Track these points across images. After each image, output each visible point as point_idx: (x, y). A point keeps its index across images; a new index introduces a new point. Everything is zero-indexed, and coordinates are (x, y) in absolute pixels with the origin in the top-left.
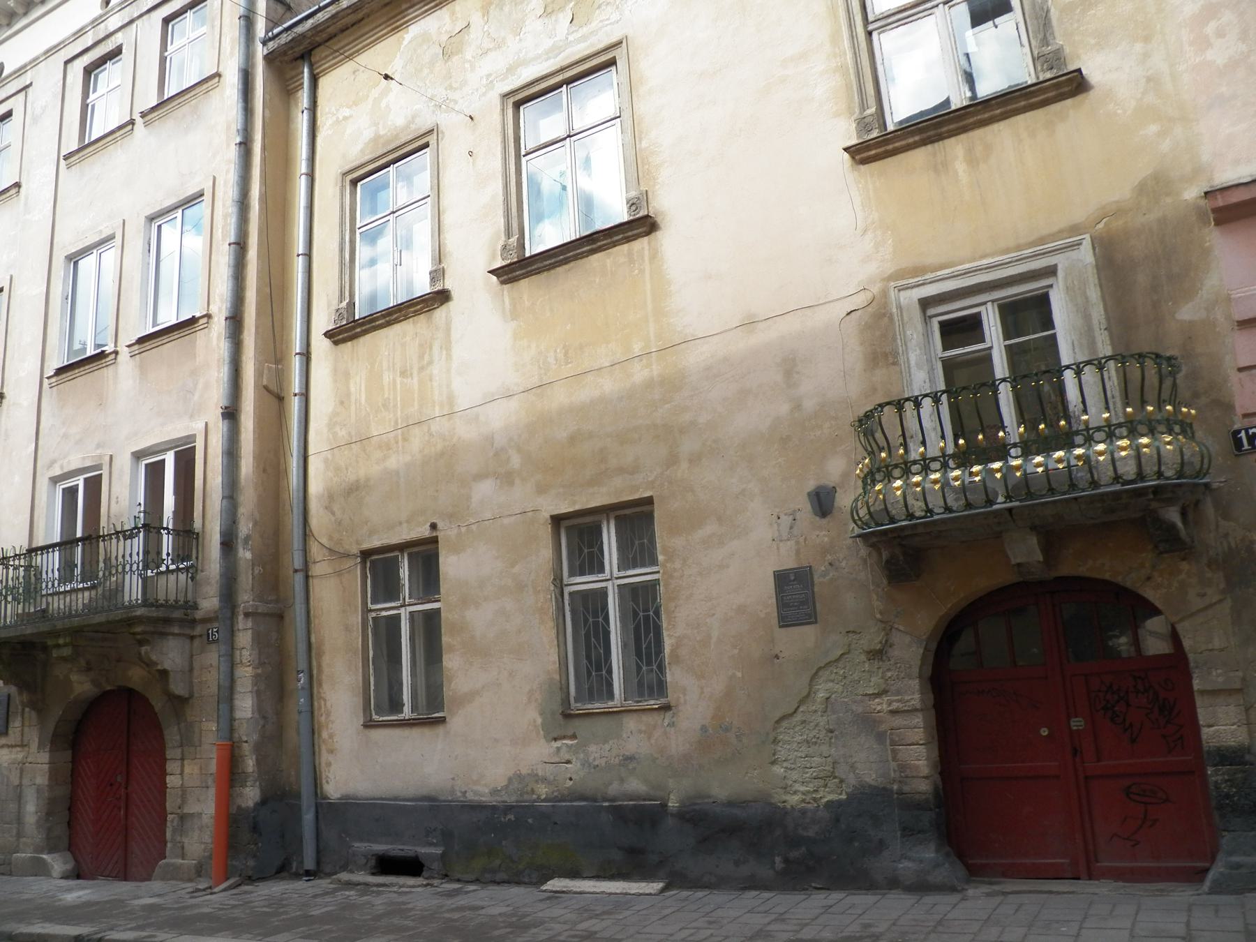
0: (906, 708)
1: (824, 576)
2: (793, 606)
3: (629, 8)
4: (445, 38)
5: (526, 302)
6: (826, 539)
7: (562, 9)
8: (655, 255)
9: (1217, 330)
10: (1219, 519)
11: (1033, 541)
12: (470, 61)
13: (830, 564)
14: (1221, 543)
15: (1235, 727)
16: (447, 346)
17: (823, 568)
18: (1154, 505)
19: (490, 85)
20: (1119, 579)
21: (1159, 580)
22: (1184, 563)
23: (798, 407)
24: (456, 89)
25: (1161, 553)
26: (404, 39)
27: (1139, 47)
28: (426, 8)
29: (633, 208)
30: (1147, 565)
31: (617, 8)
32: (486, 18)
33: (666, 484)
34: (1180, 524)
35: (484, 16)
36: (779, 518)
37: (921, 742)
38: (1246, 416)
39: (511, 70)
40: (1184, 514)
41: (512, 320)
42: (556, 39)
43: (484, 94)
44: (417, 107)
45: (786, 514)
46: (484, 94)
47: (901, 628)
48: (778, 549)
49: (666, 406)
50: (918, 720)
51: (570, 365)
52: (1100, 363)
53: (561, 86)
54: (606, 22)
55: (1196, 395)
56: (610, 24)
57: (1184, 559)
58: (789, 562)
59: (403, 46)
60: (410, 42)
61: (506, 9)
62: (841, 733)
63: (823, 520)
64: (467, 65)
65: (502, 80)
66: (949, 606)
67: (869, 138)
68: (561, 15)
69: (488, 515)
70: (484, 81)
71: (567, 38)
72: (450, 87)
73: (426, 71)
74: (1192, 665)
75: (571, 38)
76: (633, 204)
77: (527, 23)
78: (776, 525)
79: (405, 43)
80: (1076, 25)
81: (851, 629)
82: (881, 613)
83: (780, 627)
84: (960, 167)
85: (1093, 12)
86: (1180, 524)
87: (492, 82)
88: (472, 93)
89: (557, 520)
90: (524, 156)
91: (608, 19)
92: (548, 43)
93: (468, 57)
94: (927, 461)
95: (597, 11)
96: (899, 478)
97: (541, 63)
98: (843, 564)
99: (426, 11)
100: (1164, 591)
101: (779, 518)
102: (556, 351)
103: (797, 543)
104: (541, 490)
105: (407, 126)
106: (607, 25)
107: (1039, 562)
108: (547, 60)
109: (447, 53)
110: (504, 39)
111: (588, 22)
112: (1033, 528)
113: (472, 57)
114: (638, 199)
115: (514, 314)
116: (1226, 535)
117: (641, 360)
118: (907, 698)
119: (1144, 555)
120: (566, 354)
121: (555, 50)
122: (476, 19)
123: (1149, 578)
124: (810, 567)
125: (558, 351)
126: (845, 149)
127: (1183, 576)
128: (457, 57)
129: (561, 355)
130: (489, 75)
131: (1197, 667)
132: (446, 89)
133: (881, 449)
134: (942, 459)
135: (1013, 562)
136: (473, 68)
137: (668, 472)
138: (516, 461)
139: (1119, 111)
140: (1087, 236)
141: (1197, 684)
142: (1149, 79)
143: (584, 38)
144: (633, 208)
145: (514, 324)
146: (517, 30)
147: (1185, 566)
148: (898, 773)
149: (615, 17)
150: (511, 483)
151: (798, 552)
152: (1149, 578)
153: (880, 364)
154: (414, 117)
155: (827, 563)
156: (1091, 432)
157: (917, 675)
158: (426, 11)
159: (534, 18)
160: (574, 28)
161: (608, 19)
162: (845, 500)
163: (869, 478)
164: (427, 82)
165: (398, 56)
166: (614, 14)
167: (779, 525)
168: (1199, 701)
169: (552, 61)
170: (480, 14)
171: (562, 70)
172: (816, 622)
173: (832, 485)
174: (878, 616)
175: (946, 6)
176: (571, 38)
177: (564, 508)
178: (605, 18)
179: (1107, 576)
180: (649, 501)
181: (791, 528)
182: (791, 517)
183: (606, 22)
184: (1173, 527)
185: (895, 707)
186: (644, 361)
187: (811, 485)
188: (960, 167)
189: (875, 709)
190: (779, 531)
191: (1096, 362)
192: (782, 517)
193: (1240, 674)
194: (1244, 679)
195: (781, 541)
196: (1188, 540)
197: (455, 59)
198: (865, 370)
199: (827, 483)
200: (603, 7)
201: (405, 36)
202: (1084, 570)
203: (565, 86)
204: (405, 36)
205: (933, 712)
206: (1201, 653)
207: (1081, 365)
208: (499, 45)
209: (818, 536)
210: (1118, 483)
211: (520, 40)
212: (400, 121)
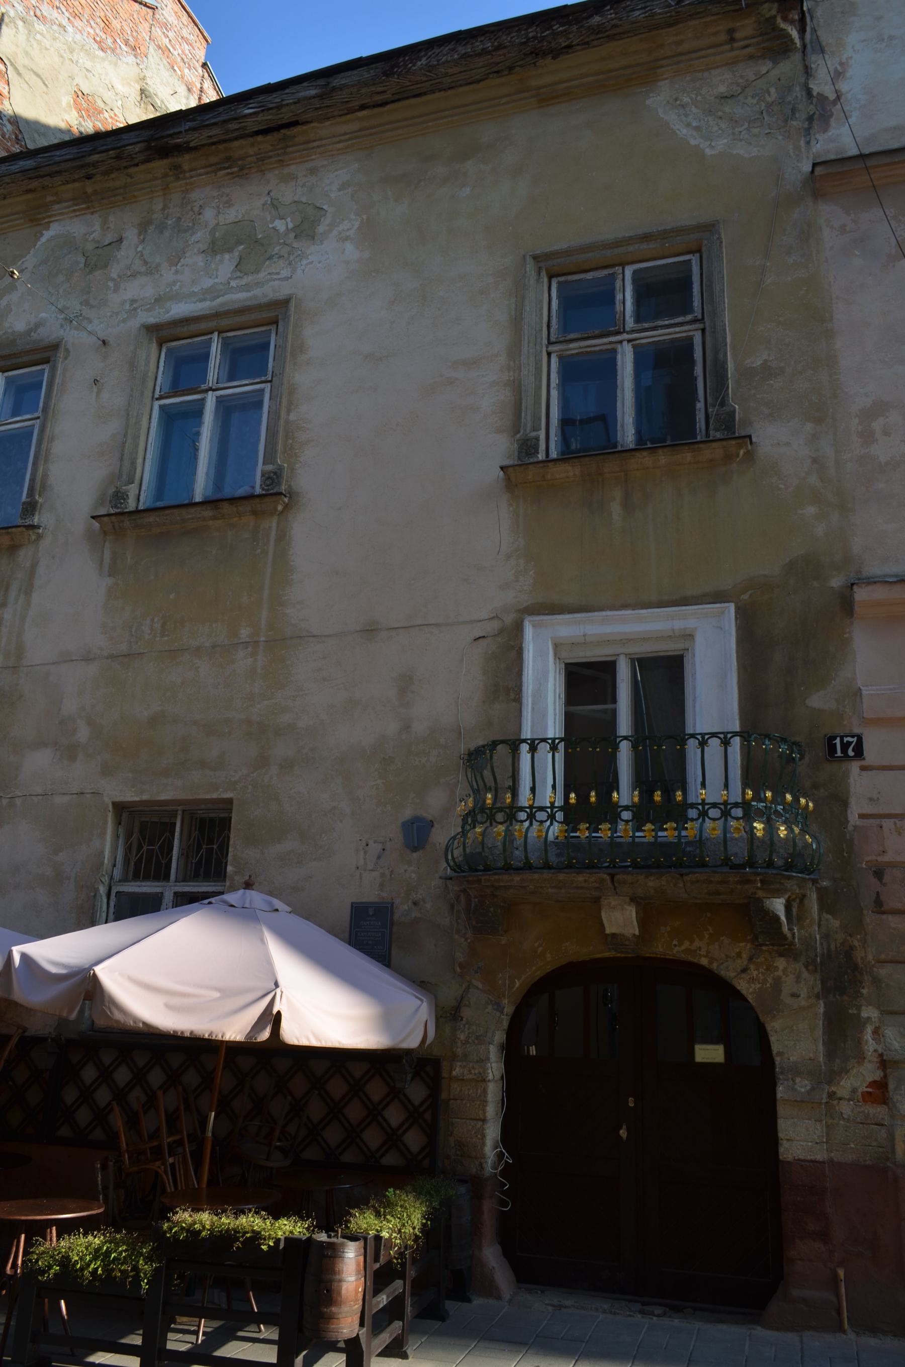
3: (303, 267)
4: (90, 247)
5: (129, 560)
6: (414, 875)
7: (230, 250)
8: (283, 537)
9: (845, 723)
11: (631, 912)
12: (113, 280)
13: (415, 904)
16: (28, 590)
17: (406, 907)
18: (760, 894)
19: (132, 313)
20: (714, 966)
21: (755, 973)
22: (782, 959)
23: (407, 728)
24: (92, 307)
26: (42, 235)
27: (809, 426)
28: (76, 208)
29: (268, 482)
30: (744, 956)
31: (290, 264)
32: (142, 237)
33: (250, 787)
34: (783, 918)
35: (140, 234)
36: (367, 845)
38: (862, 816)
39: (159, 300)
40: (788, 908)
41: (110, 576)
42: (216, 280)
43: (124, 321)
44: (44, 315)
45: (375, 842)
46: (124, 321)
47: (480, 986)
48: (361, 878)
49: (266, 702)
51: (166, 638)
52: (725, 737)
53: (212, 333)
54: (275, 277)
55: (816, 786)
56: (279, 279)
57: (781, 955)
58: (370, 893)
59: (39, 243)
60: (48, 240)
61: (167, 233)
63: (415, 855)
64: (111, 284)
65: (149, 310)
67: (529, 462)
68: (227, 256)
69: (39, 790)
70: (127, 306)
71: (229, 283)
72: (86, 303)
73: (61, 278)
75: (233, 284)
76: (269, 478)
77: (187, 255)
78: (362, 853)
79: (43, 240)
80: (753, 391)
84: (616, 509)
85: (772, 382)
86: (783, 918)
87: (135, 309)
88: (111, 316)
89: (120, 808)
90: (157, 399)
91: (278, 274)
92: (207, 283)
93: (114, 275)
94: (534, 810)
95: (267, 263)
96: (501, 823)
97: (195, 303)
98: (428, 906)
99: (75, 211)
100: (758, 986)
101: (367, 845)
102: (153, 620)
103: (383, 875)
104: (107, 771)
105: (28, 332)
106: (276, 279)
107: (634, 935)
108: (205, 300)
109: (91, 266)
110: (158, 266)
111: (257, 271)
112: (633, 900)
113: (119, 277)
114: (275, 473)
115: (113, 572)
117: (247, 648)
119: (741, 944)
120: (164, 625)
121: (211, 293)
122: (131, 235)
123: (745, 970)
124: (392, 904)
125: (156, 620)
126: (502, 468)
127: (780, 973)
128: (100, 272)
129: (158, 626)
130: (133, 301)
131: (782, 1073)
132: (81, 304)
133: (488, 789)
134: (549, 810)
135: (608, 931)
136: (116, 289)
137: (255, 774)
138: (83, 734)
139: (782, 486)
140: (732, 606)
142: (815, 460)
143: (246, 288)
144: (268, 482)
145: (110, 581)
146: (175, 260)
147: (781, 963)
149: (285, 273)
150: (73, 758)
151: (382, 885)
152: (745, 970)
153: (501, 698)
154: (37, 326)
155: (410, 903)
156: (707, 807)
158: (75, 211)
159: (195, 251)
160: (239, 274)
161: (278, 274)
162: (440, 837)
163: (470, 818)
164: (61, 291)
165: (32, 252)
166: (285, 270)
167: (365, 853)
168: (781, 1110)
169: (207, 304)
170: (136, 231)
171: (217, 315)
173: (430, 818)
175: (630, 344)
176: (233, 284)
177: (130, 796)
178: (274, 271)
179: (704, 962)
180: (230, 801)
181: (379, 857)
182: (380, 847)
183: (275, 277)
184: (777, 918)
186: (250, 649)
187: (408, 813)
188: (616, 509)
190: (365, 859)
191: (722, 736)
192: (371, 843)
195: (365, 870)
196: (789, 935)
197: (98, 273)
198: (484, 702)
199: (425, 815)
200: (275, 259)
201: (44, 232)
202: (679, 950)
203: (216, 334)
204: (44, 232)
207: (707, 737)
208: (152, 270)
209: (405, 871)
210: (727, 865)
211: (177, 272)
212: (20, 326)
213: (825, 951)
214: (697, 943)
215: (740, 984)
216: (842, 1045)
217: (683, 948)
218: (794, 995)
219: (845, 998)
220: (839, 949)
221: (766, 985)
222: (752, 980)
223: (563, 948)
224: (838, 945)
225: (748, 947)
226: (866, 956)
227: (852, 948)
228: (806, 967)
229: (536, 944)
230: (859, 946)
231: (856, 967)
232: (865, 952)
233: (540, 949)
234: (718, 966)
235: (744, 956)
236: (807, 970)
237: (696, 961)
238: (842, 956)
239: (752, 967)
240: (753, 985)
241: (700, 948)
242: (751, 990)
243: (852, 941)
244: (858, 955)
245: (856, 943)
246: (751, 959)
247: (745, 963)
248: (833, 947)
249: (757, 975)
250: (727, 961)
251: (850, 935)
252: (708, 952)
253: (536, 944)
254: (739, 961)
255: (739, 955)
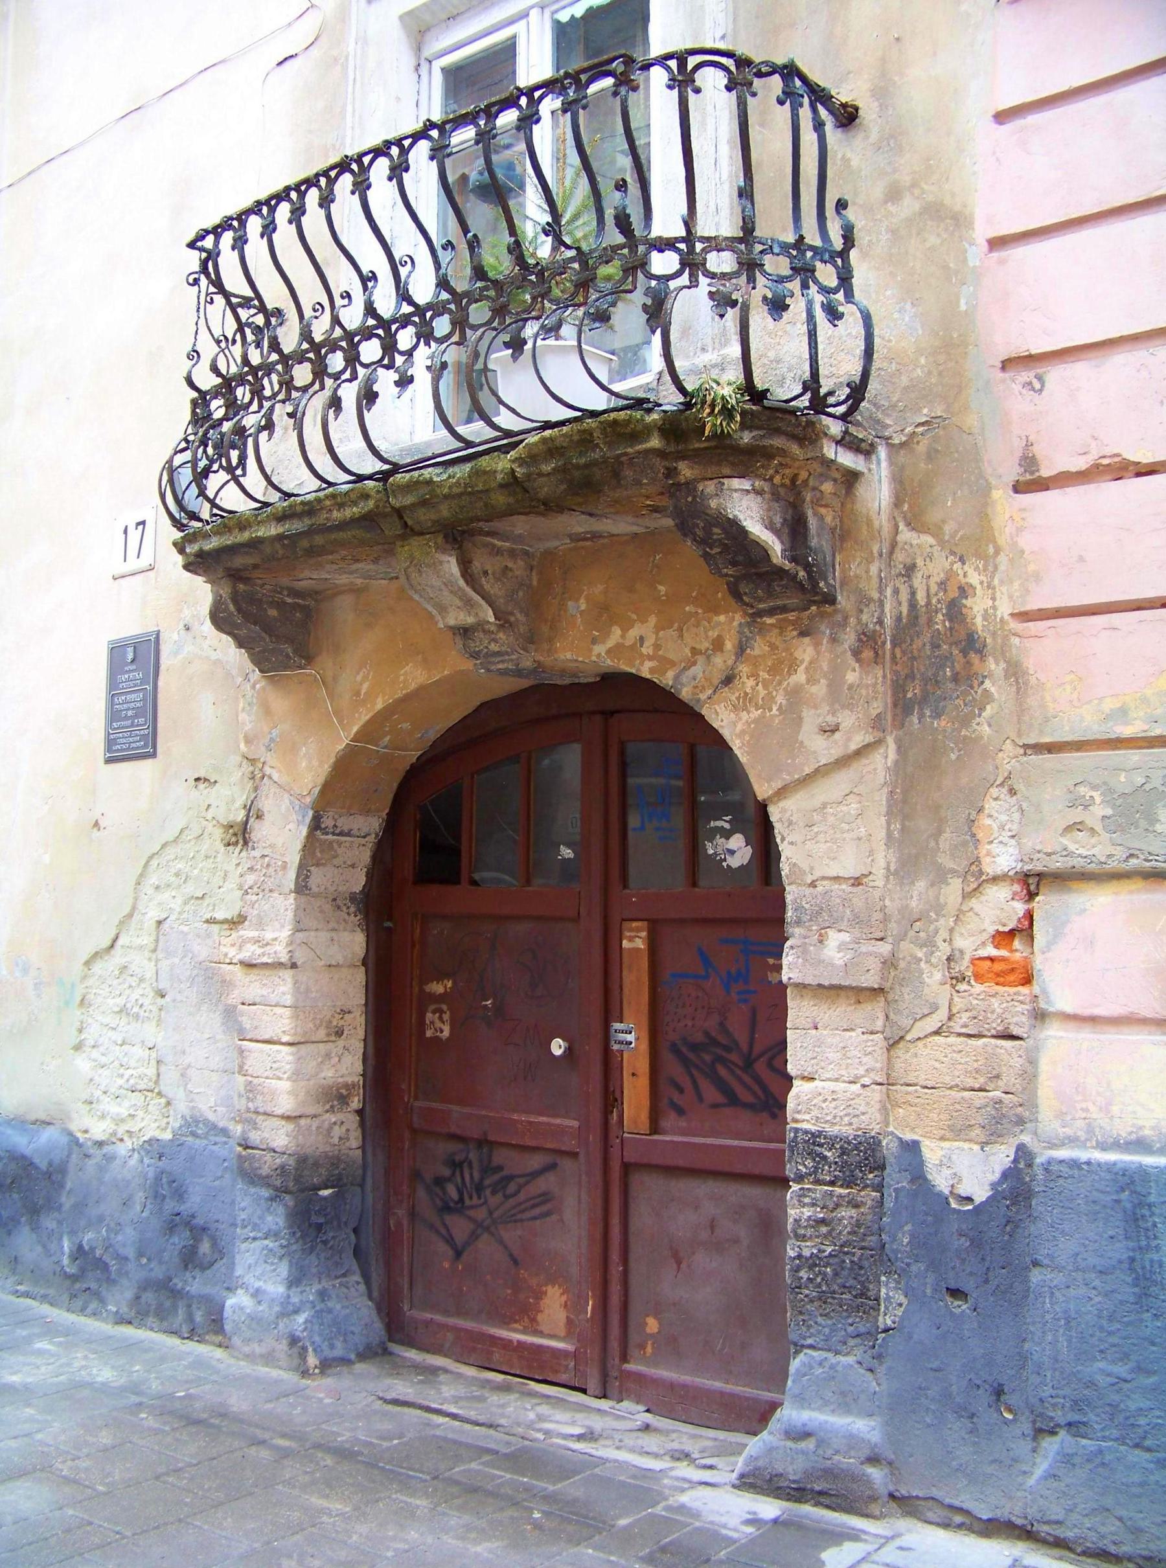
0: (265, 960)
1: (176, 654)
2: (126, 718)
10: (902, 526)
14: (896, 591)
15: (856, 1088)
20: (667, 679)
21: (750, 683)
25: (760, 614)
30: (729, 645)
37: (285, 1039)
47: (275, 777)
50: (283, 988)
62: (174, 1001)
66: (355, 729)
74: (789, 914)
81: (202, 775)
82: (248, 741)
83: (109, 761)
100: (756, 714)
116: (910, 570)
118: (269, 935)
119: (722, 618)
124: (158, 634)
127: (800, 677)
131: (798, 922)
141: (792, 968)
147: (805, 651)
148: (244, 1101)
152: (728, 680)
155: (181, 626)
157: (292, 887)
168: (798, 1011)
172: (153, 755)
174: (242, 746)
185: (248, 954)
189: (226, 955)
193: (885, 948)
194: (890, 963)
205: (360, 976)
206: (813, 885)
213: (905, 610)
214: (634, 633)
215: (717, 714)
216: (932, 844)
217: (610, 643)
218: (830, 730)
219: (943, 723)
220: (934, 601)
221: (770, 710)
222: (747, 701)
223: (402, 678)
224: (934, 588)
225: (735, 624)
226: (994, 608)
227: (964, 591)
228: (856, 653)
229: (359, 678)
230: (982, 583)
231: (971, 644)
232: (994, 599)
233: (365, 686)
234: (677, 678)
235: (729, 645)
236: (858, 660)
237: (634, 671)
238: (940, 616)
239: (744, 669)
240: (744, 715)
241: (642, 639)
242: (739, 727)
243: (965, 575)
244: (977, 607)
245: (974, 578)
246: (741, 650)
247: (730, 662)
248: (921, 597)
249: (753, 689)
250: (694, 663)
251: (962, 560)
252: (657, 647)
253: (359, 678)
254: (718, 660)
255: (718, 645)
